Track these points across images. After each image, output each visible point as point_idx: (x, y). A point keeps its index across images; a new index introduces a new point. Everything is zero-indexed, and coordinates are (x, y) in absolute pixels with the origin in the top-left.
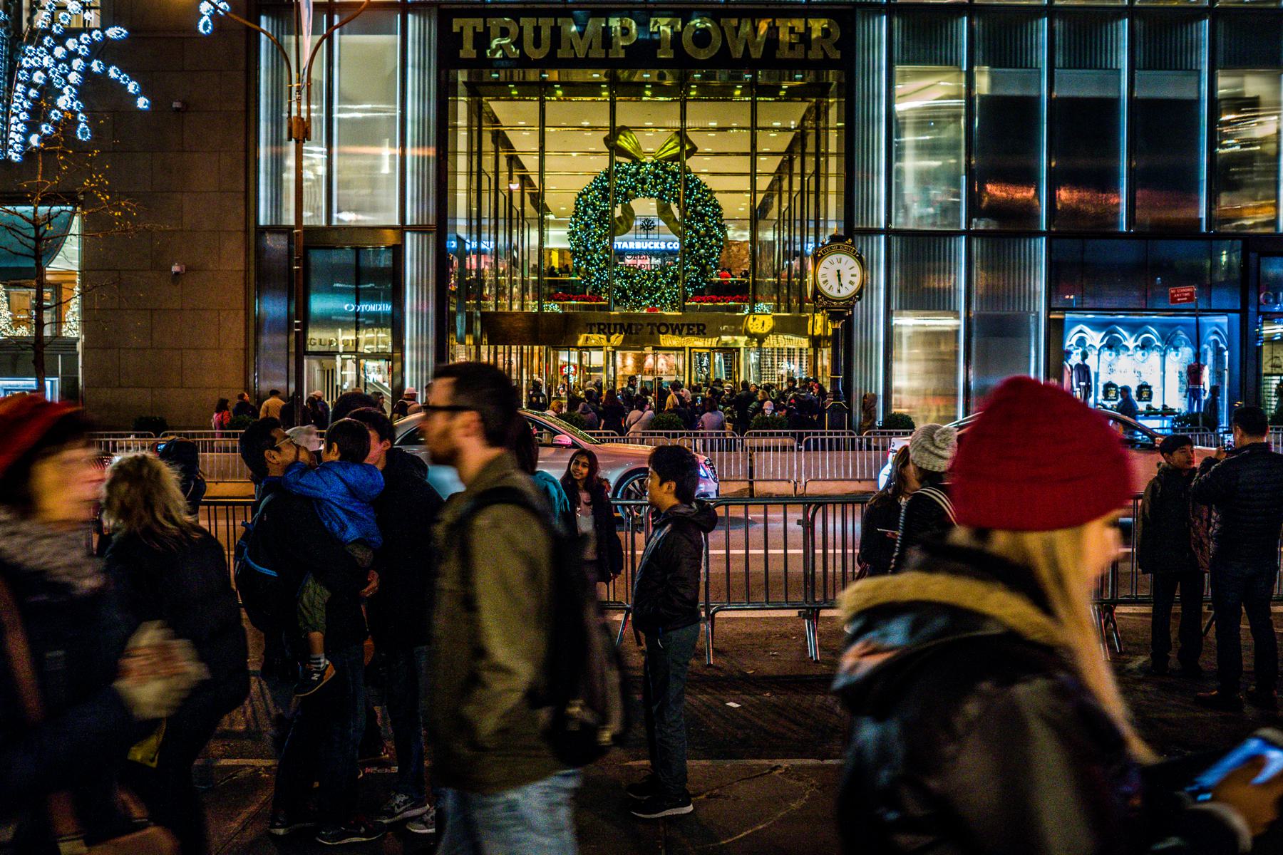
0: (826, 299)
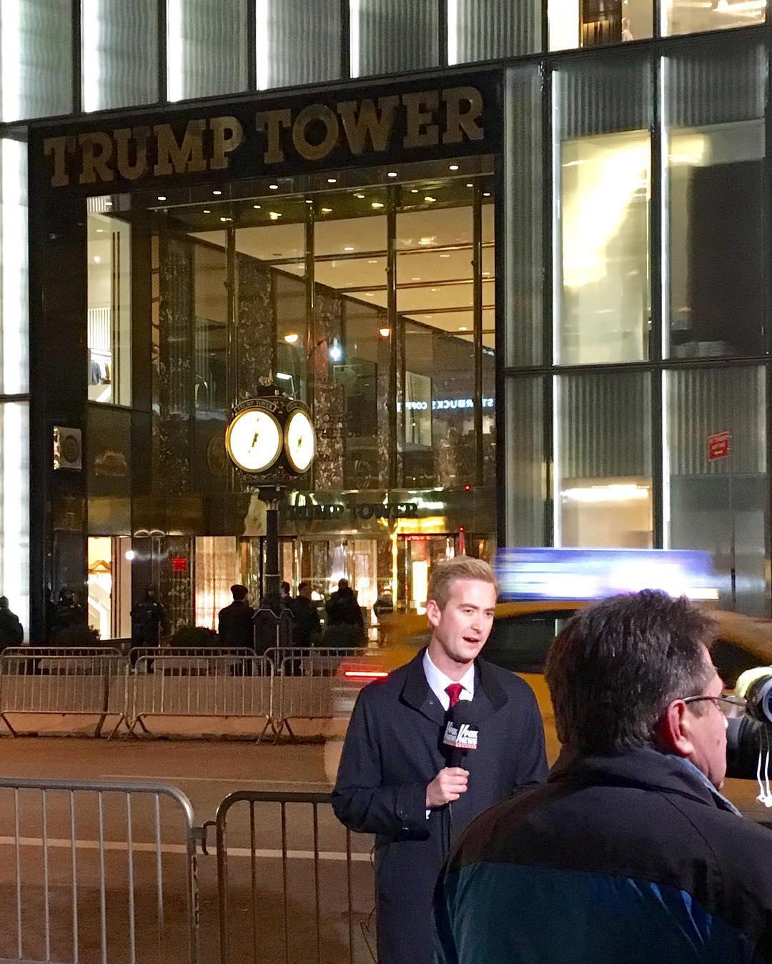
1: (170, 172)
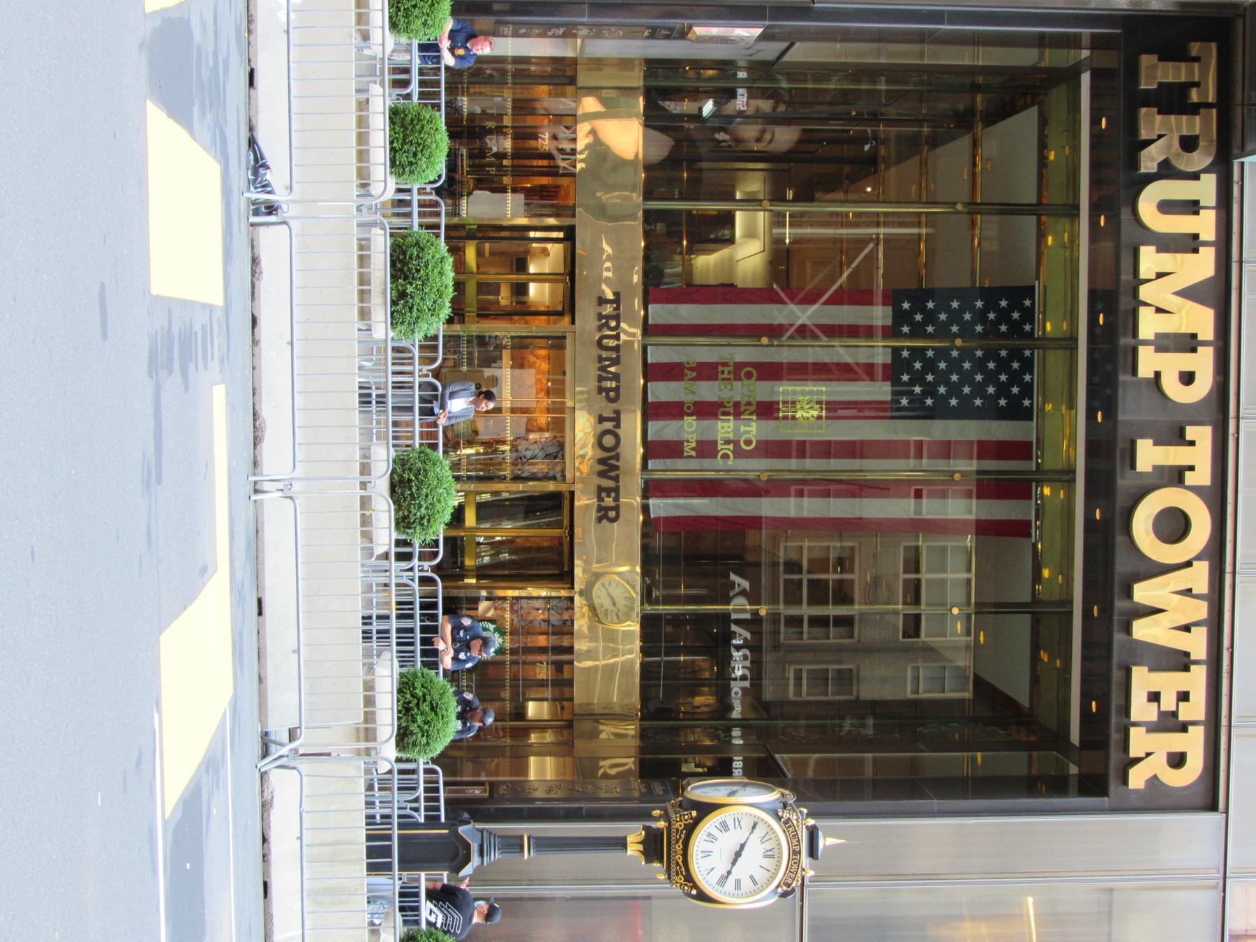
0: (691, 829)
1: (1143, 275)
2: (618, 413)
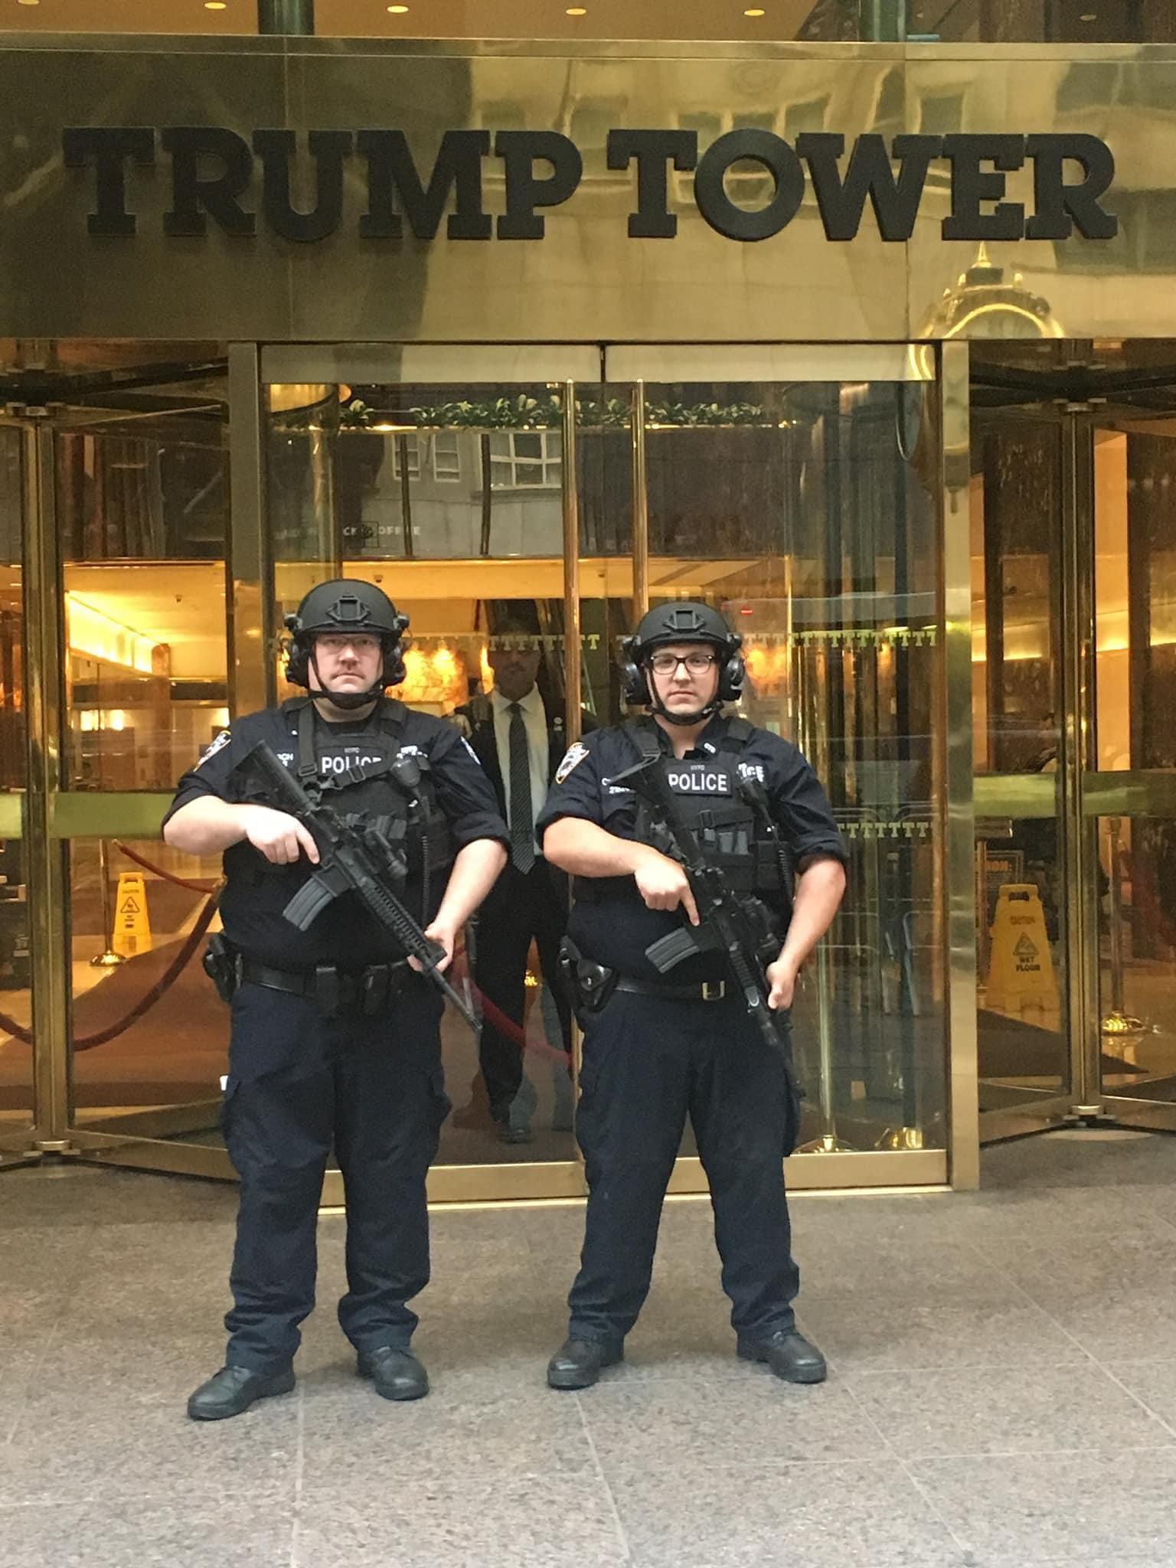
2: (624, 147)
